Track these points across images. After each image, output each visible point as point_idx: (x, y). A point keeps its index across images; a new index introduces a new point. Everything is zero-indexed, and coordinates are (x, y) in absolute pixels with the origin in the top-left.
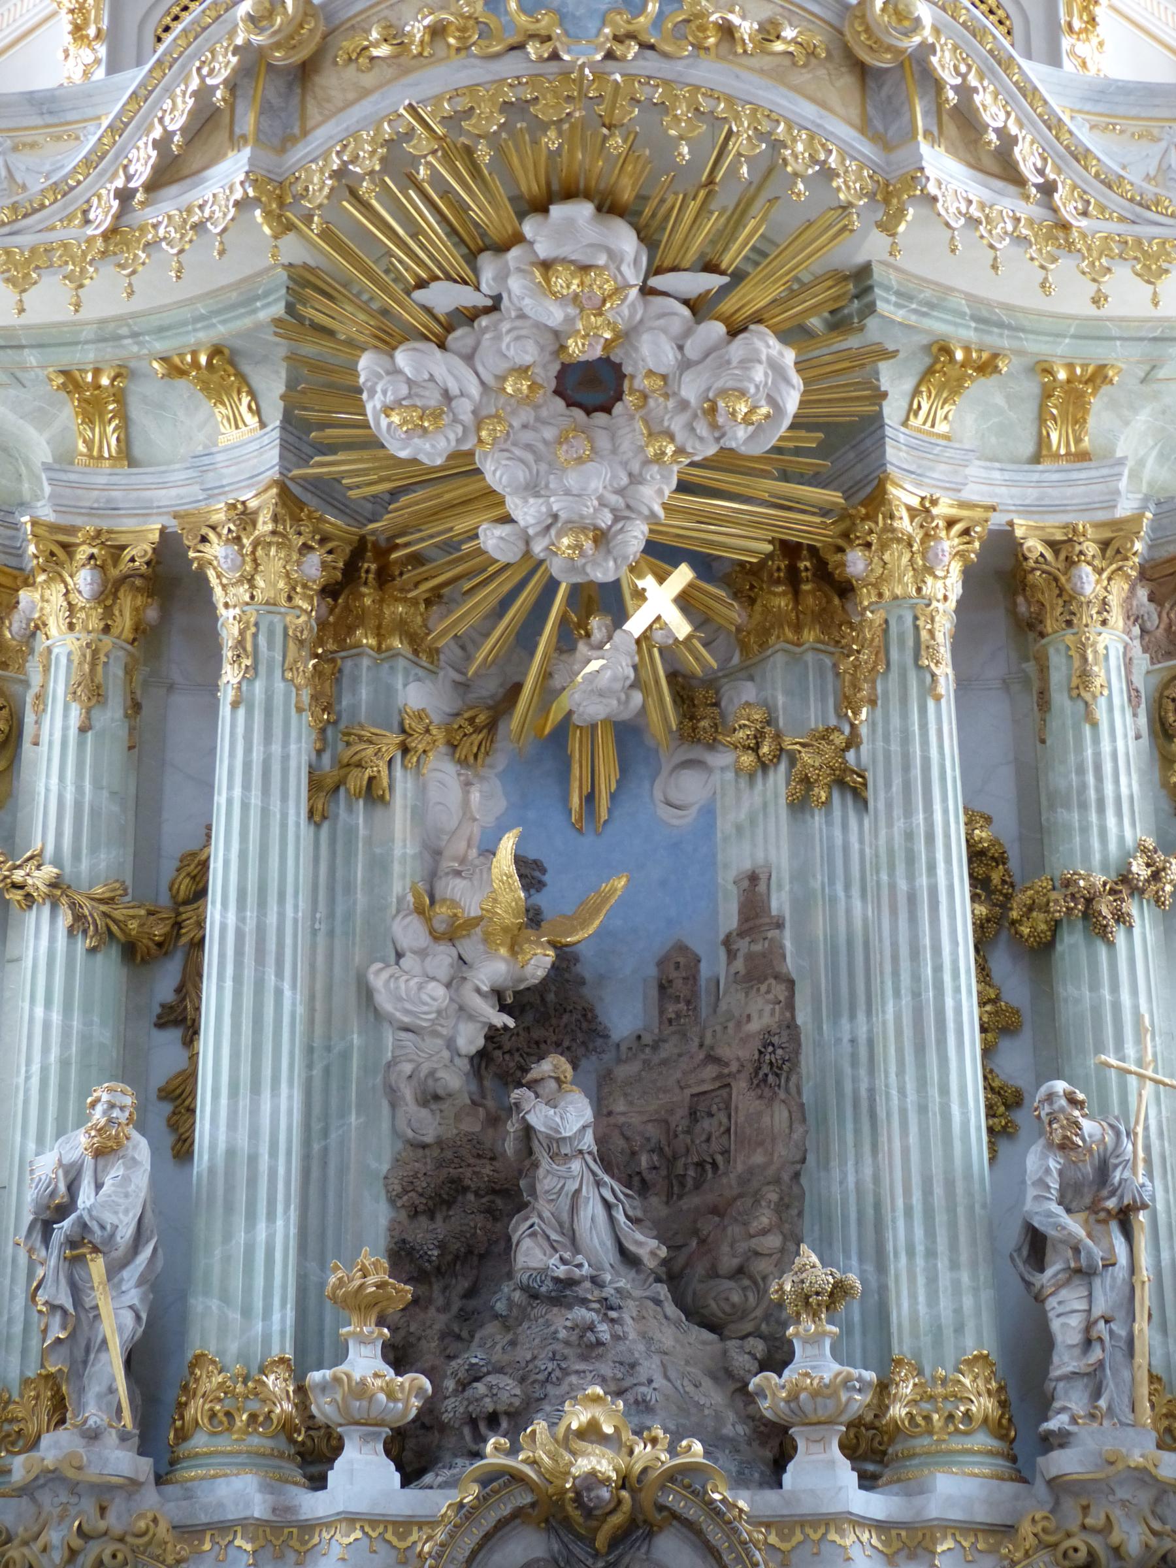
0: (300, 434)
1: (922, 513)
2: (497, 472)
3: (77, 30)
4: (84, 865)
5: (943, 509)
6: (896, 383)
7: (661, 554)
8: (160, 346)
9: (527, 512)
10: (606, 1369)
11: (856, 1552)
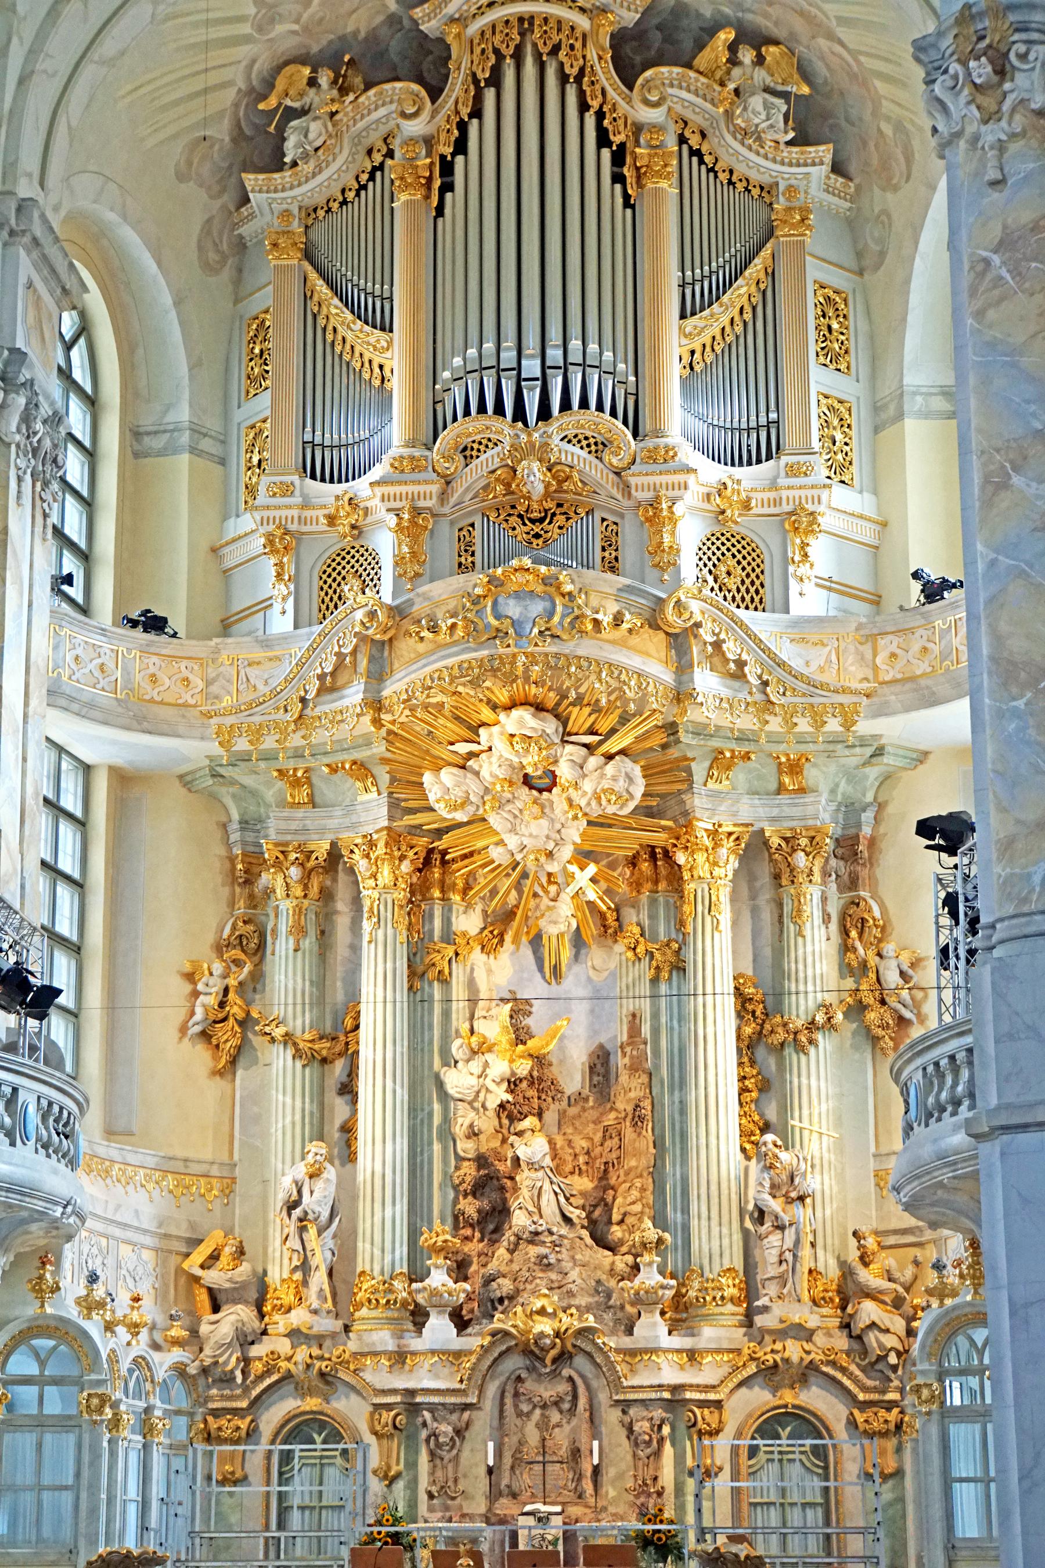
0: (395, 807)
1: (713, 834)
2: (495, 820)
3: (279, 576)
4: (299, 1022)
5: (727, 828)
6: (699, 770)
7: (584, 856)
8: (327, 760)
9: (512, 842)
10: (553, 1276)
11: (664, 1365)
